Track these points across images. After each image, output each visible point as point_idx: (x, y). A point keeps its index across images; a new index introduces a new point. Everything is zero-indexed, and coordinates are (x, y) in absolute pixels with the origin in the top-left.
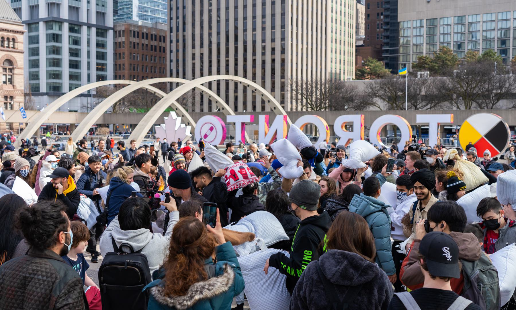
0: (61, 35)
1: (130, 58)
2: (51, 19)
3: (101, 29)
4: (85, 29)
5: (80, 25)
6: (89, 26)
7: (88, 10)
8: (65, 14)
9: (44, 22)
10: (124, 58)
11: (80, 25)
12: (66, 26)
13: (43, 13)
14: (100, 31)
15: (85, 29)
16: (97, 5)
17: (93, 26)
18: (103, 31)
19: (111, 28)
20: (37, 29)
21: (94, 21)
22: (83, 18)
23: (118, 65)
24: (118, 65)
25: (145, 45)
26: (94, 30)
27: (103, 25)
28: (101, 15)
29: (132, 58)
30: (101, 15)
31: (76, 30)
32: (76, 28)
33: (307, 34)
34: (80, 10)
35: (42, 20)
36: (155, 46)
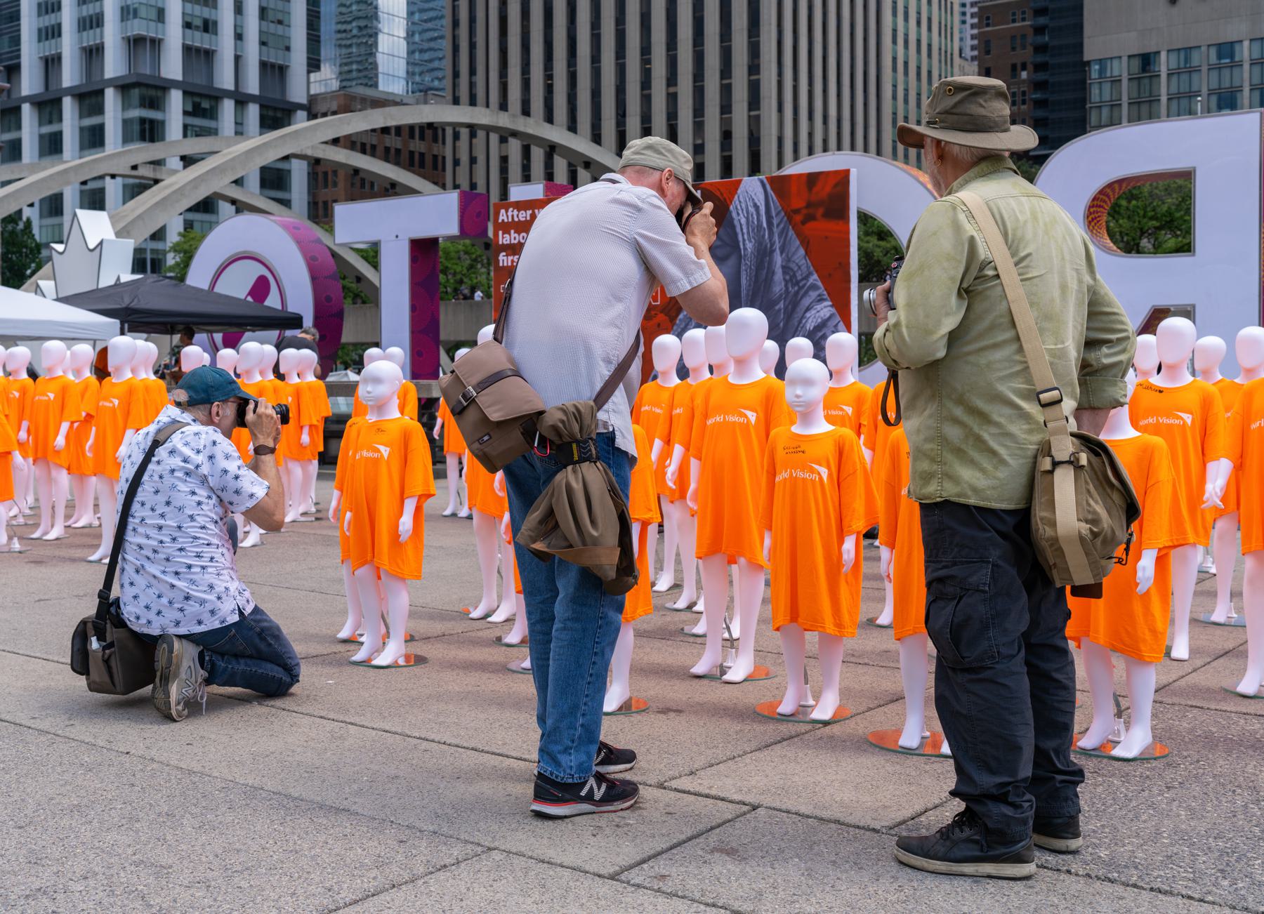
0: (163, 123)
1: (352, 184)
2: (134, 80)
3: (275, 109)
4: (228, 106)
5: (217, 96)
6: (242, 101)
7: (237, 58)
8: (172, 66)
9: (116, 87)
10: (335, 184)
11: (217, 96)
12: (176, 100)
13: (114, 65)
14: (271, 113)
15: (228, 106)
16: (263, 43)
17: (252, 98)
18: (279, 115)
19: (300, 107)
20: (100, 110)
21: (252, 85)
22: (225, 79)
23: (321, 205)
24: (321, 205)
25: (393, 151)
26: (253, 111)
27: (278, 96)
28: (274, 72)
29: (358, 184)
30: (274, 72)
31: (205, 110)
32: (205, 104)
33: (825, 91)
34: (217, 58)
35: (112, 82)
36: (422, 155)
